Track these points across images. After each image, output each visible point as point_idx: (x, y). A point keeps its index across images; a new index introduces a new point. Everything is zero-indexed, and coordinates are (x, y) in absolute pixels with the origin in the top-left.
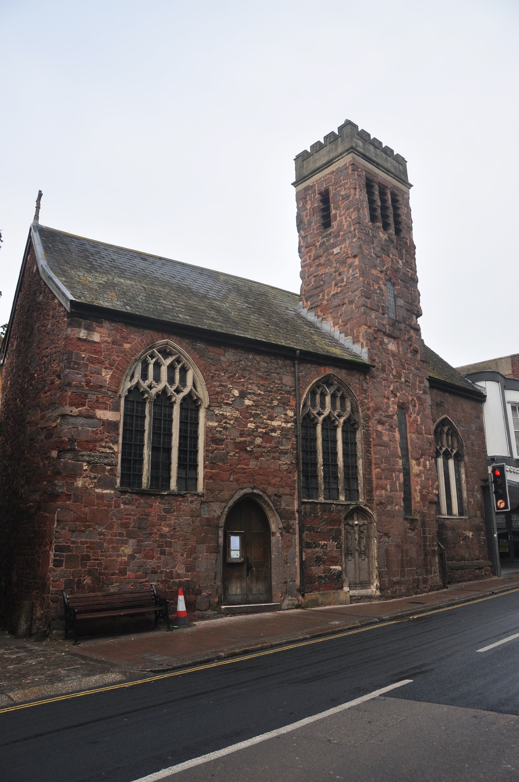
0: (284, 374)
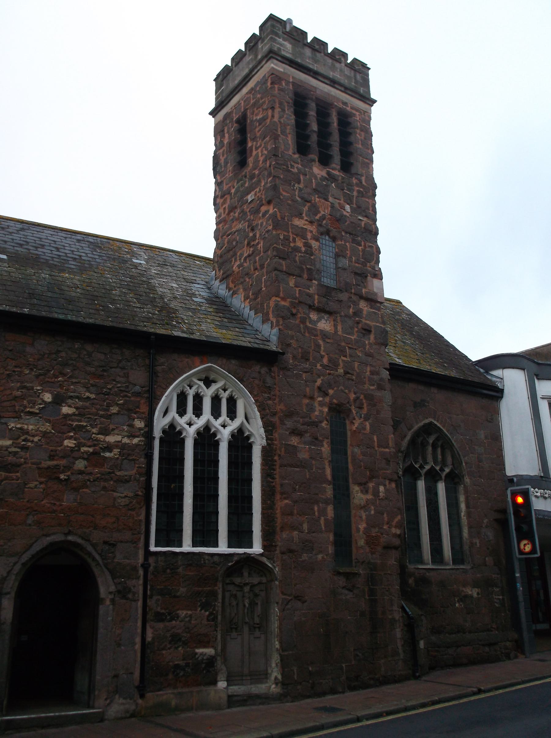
0: (132, 369)
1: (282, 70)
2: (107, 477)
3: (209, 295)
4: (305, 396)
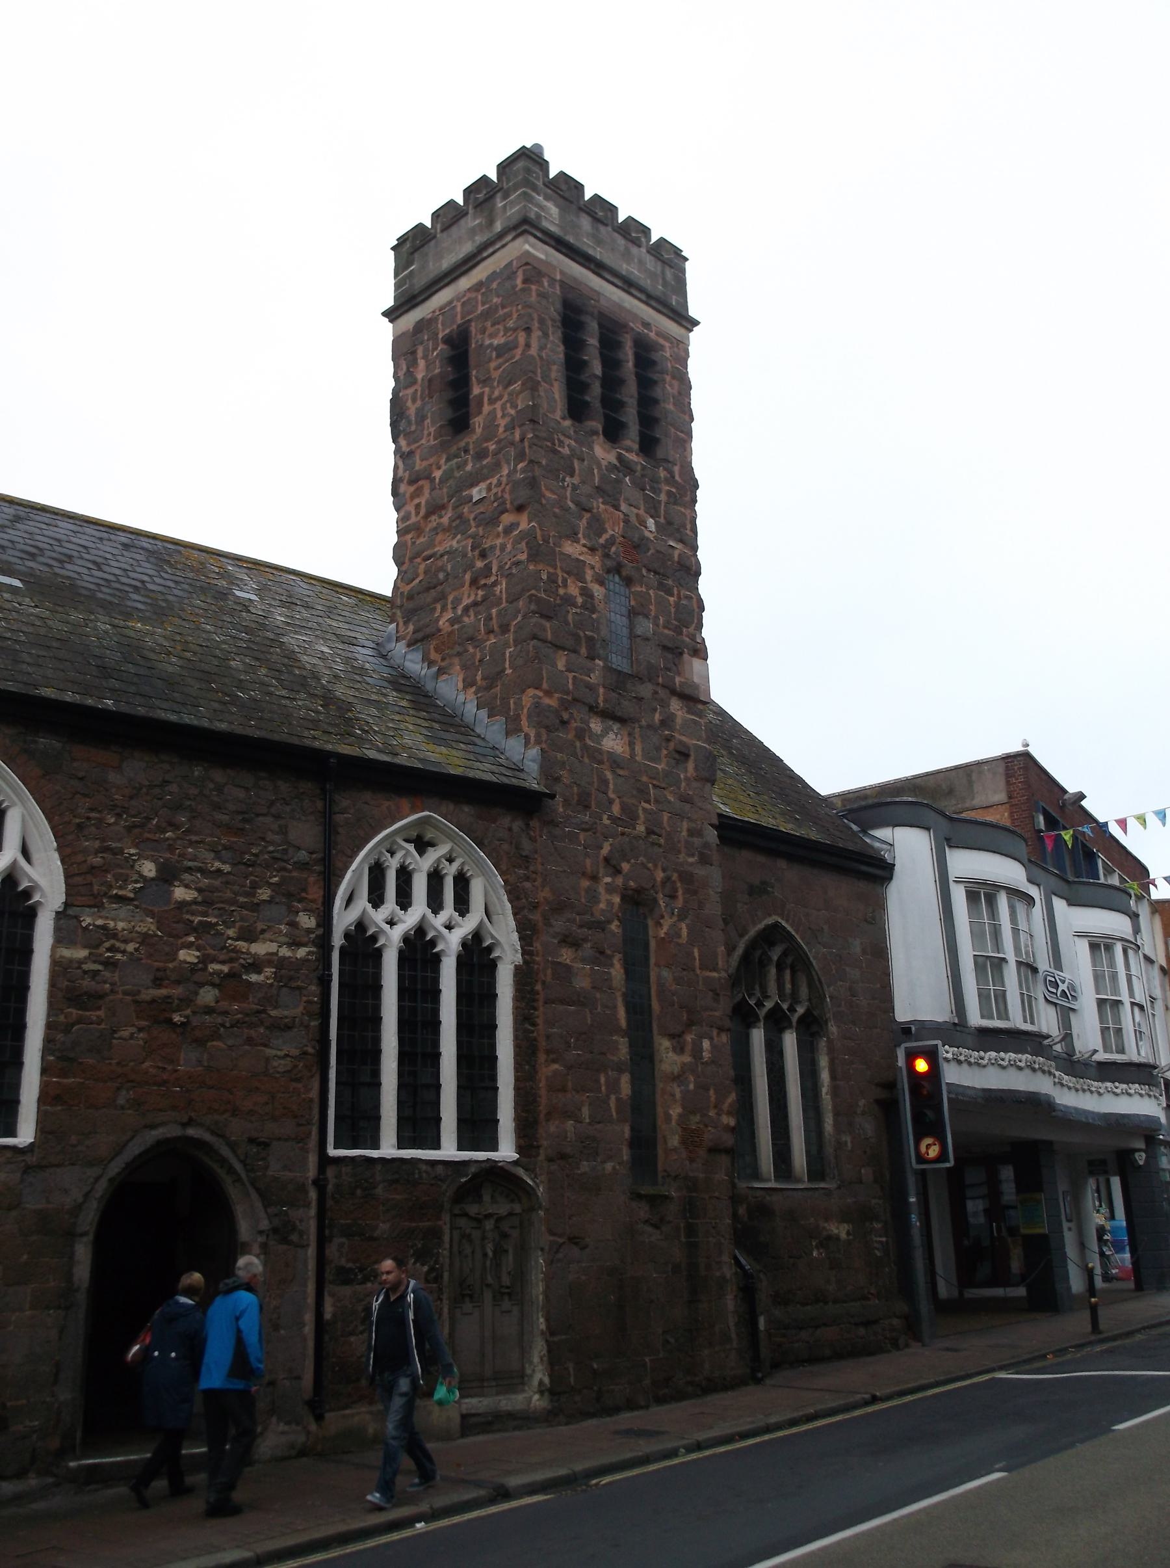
1: (542, 257)
2: (254, 1019)
4: (584, 874)
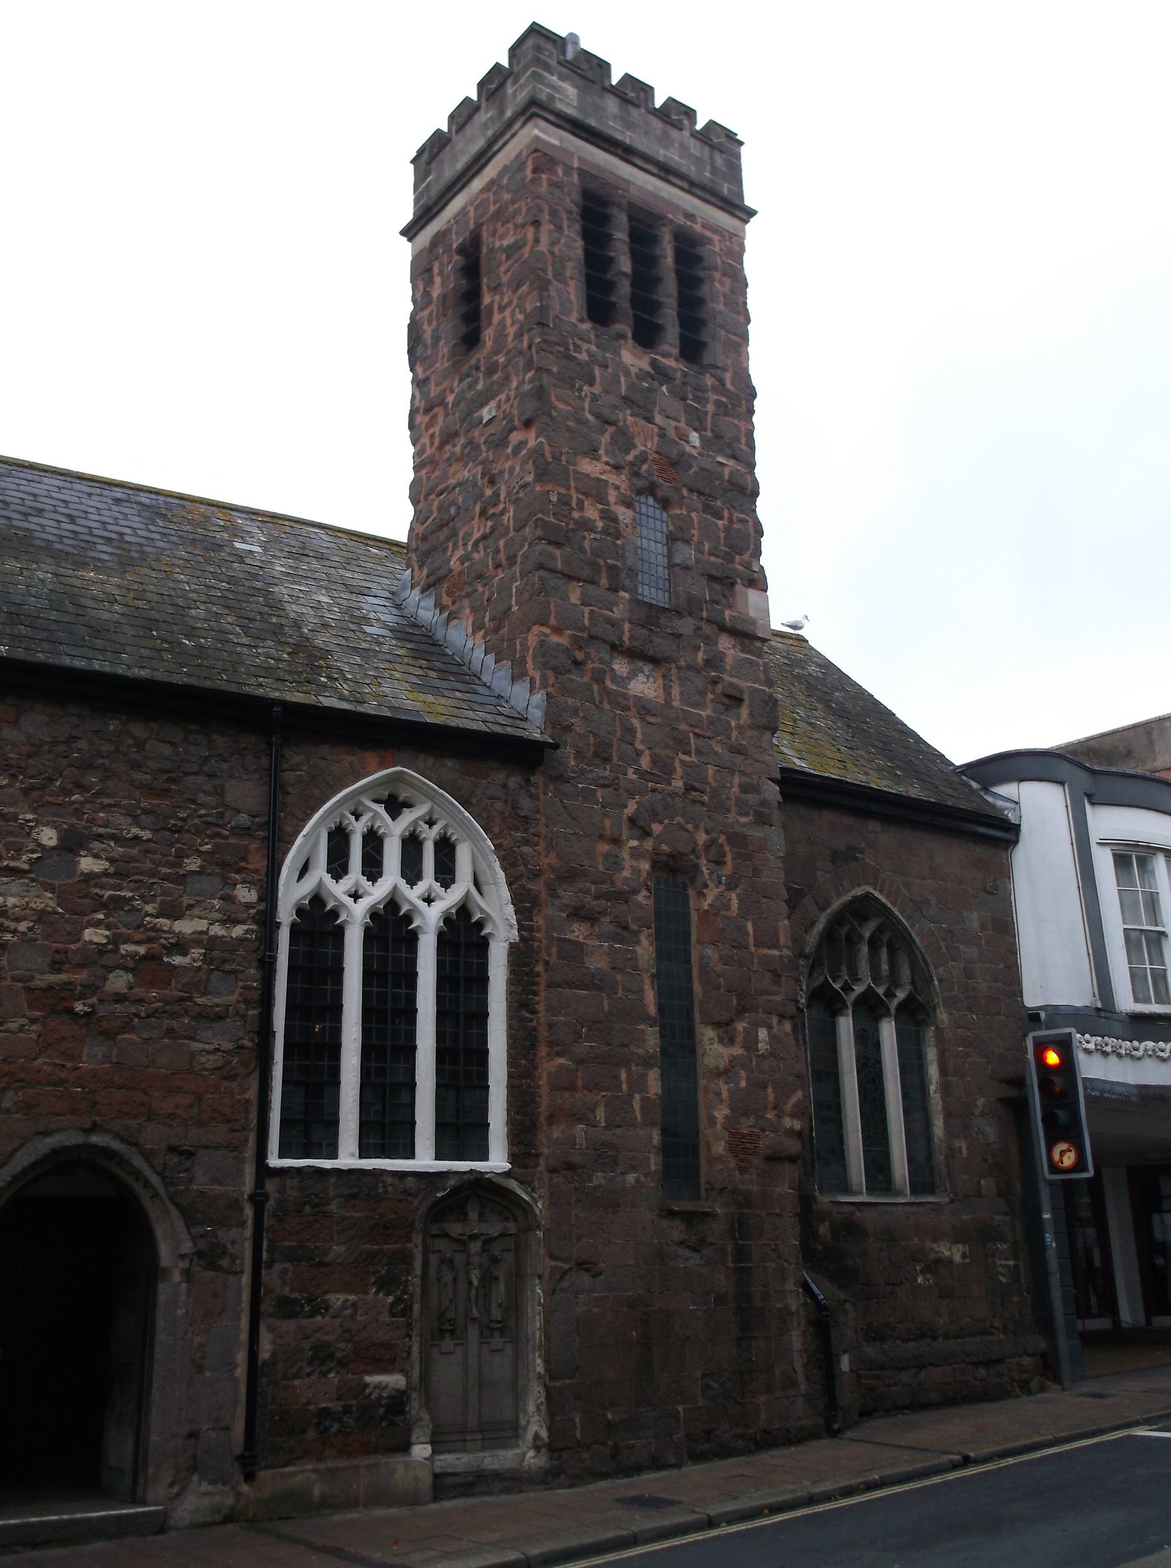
0: (232, 777)
1: (556, 142)
2: (176, 1008)
3: (399, 620)
4: (601, 837)
